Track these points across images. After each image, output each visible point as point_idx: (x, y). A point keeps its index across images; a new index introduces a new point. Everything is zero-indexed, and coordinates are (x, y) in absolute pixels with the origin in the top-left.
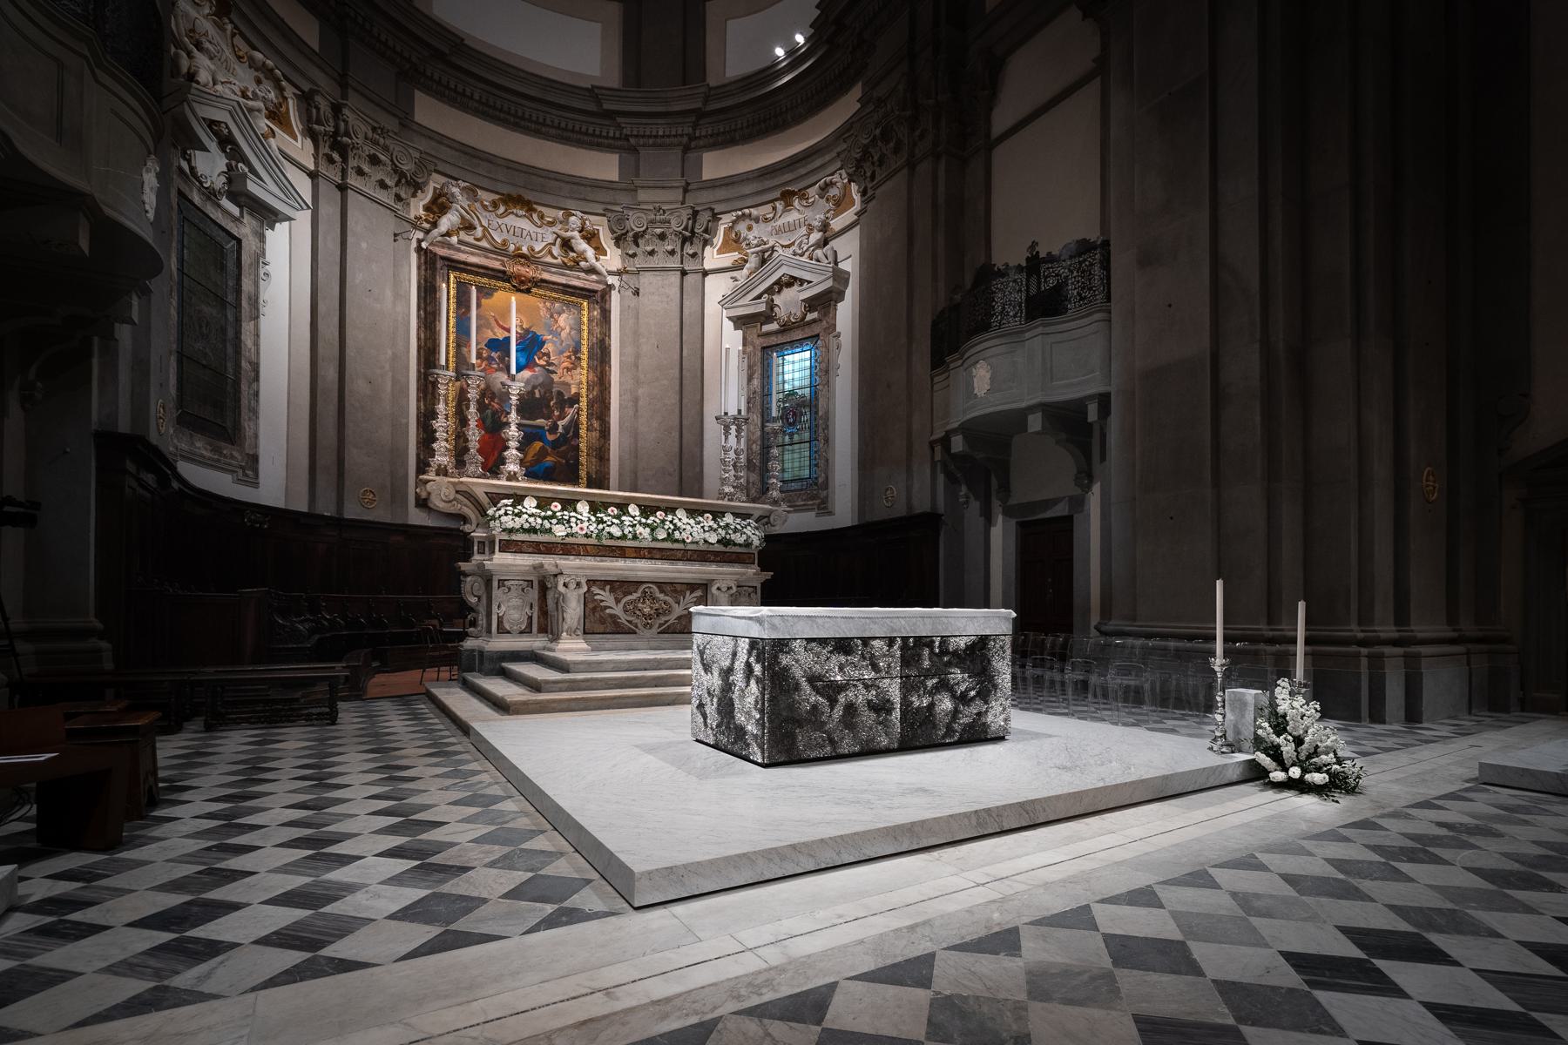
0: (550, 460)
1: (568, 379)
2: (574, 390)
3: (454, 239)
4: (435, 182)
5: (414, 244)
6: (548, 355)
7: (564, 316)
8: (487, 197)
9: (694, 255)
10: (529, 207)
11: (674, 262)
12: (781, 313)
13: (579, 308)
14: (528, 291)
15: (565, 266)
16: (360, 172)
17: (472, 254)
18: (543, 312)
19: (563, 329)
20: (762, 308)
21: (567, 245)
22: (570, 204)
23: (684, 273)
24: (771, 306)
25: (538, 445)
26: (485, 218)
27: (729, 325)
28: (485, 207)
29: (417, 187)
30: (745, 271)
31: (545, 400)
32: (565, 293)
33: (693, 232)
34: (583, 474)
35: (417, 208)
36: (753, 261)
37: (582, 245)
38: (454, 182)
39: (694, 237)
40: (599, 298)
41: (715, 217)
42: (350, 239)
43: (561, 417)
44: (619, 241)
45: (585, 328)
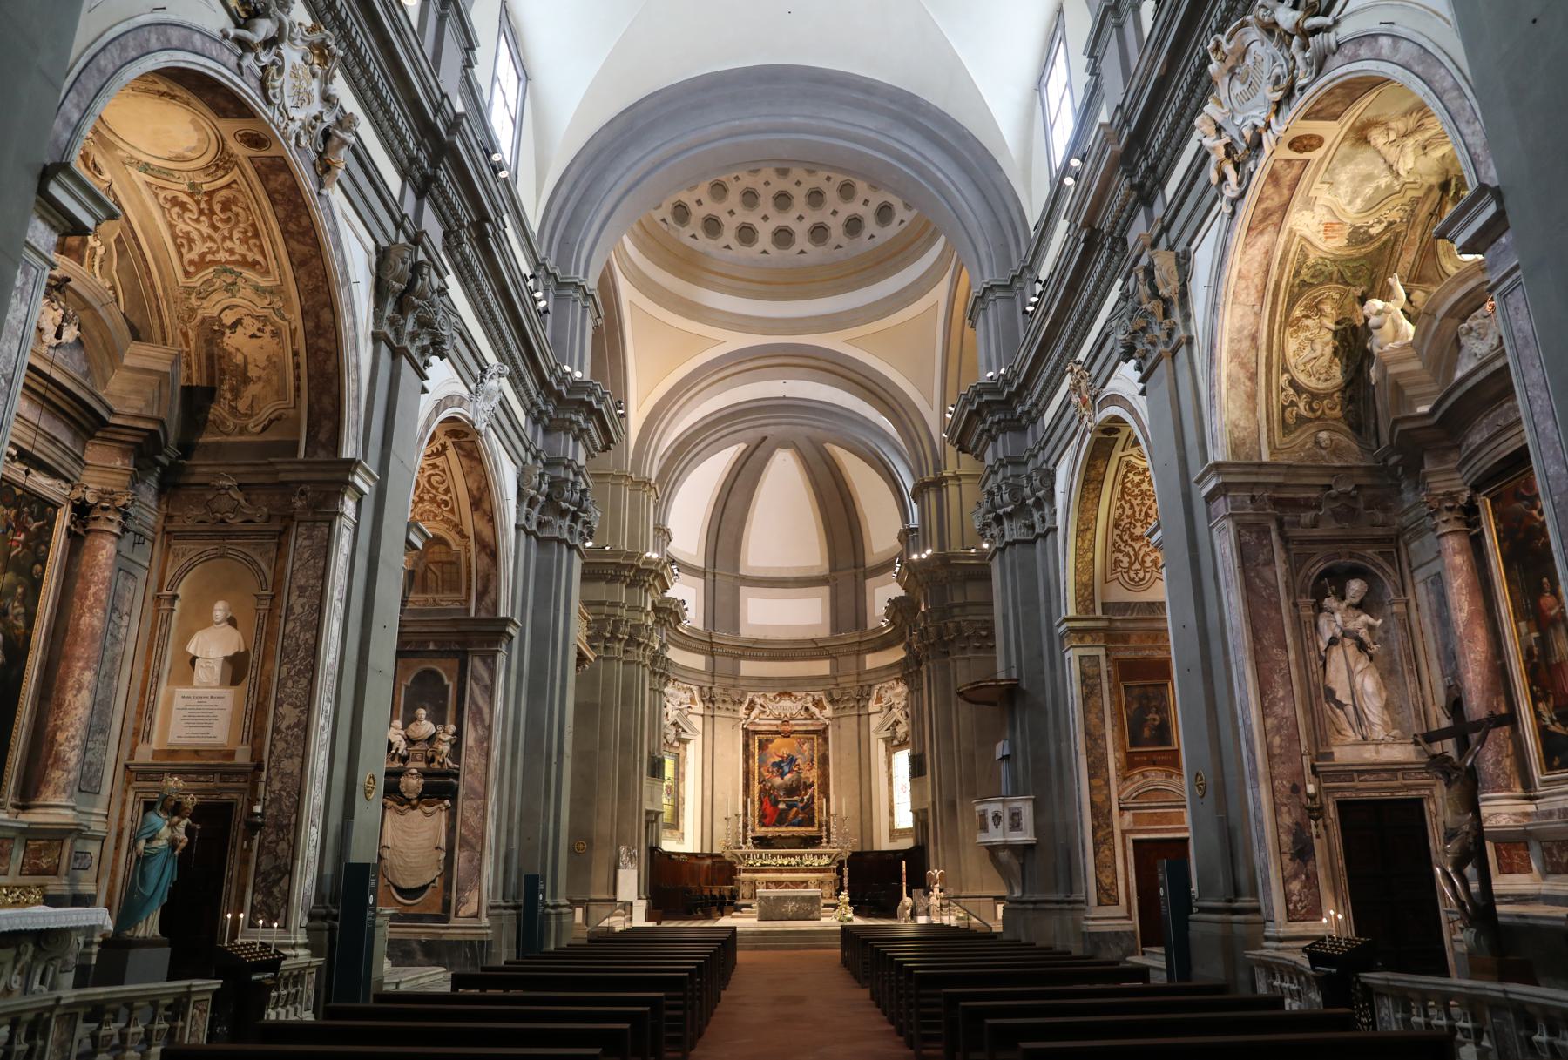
0: (800, 816)
4: (750, 696)
8: (770, 695)
10: (790, 695)
11: (855, 712)
12: (899, 735)
18: (796, 745)
20: (889, 734)
21: (807, 709)
26: (770, 706)
27: (881, 741)
29: (741, 703)
30: (882, 715)
31: (798, 787)
35: (742, 711)
36: (885, 710)
37: (813, 709)
39: (863, 697)
40: (822, 733)
41: (871, 686)
44: (832, 702)
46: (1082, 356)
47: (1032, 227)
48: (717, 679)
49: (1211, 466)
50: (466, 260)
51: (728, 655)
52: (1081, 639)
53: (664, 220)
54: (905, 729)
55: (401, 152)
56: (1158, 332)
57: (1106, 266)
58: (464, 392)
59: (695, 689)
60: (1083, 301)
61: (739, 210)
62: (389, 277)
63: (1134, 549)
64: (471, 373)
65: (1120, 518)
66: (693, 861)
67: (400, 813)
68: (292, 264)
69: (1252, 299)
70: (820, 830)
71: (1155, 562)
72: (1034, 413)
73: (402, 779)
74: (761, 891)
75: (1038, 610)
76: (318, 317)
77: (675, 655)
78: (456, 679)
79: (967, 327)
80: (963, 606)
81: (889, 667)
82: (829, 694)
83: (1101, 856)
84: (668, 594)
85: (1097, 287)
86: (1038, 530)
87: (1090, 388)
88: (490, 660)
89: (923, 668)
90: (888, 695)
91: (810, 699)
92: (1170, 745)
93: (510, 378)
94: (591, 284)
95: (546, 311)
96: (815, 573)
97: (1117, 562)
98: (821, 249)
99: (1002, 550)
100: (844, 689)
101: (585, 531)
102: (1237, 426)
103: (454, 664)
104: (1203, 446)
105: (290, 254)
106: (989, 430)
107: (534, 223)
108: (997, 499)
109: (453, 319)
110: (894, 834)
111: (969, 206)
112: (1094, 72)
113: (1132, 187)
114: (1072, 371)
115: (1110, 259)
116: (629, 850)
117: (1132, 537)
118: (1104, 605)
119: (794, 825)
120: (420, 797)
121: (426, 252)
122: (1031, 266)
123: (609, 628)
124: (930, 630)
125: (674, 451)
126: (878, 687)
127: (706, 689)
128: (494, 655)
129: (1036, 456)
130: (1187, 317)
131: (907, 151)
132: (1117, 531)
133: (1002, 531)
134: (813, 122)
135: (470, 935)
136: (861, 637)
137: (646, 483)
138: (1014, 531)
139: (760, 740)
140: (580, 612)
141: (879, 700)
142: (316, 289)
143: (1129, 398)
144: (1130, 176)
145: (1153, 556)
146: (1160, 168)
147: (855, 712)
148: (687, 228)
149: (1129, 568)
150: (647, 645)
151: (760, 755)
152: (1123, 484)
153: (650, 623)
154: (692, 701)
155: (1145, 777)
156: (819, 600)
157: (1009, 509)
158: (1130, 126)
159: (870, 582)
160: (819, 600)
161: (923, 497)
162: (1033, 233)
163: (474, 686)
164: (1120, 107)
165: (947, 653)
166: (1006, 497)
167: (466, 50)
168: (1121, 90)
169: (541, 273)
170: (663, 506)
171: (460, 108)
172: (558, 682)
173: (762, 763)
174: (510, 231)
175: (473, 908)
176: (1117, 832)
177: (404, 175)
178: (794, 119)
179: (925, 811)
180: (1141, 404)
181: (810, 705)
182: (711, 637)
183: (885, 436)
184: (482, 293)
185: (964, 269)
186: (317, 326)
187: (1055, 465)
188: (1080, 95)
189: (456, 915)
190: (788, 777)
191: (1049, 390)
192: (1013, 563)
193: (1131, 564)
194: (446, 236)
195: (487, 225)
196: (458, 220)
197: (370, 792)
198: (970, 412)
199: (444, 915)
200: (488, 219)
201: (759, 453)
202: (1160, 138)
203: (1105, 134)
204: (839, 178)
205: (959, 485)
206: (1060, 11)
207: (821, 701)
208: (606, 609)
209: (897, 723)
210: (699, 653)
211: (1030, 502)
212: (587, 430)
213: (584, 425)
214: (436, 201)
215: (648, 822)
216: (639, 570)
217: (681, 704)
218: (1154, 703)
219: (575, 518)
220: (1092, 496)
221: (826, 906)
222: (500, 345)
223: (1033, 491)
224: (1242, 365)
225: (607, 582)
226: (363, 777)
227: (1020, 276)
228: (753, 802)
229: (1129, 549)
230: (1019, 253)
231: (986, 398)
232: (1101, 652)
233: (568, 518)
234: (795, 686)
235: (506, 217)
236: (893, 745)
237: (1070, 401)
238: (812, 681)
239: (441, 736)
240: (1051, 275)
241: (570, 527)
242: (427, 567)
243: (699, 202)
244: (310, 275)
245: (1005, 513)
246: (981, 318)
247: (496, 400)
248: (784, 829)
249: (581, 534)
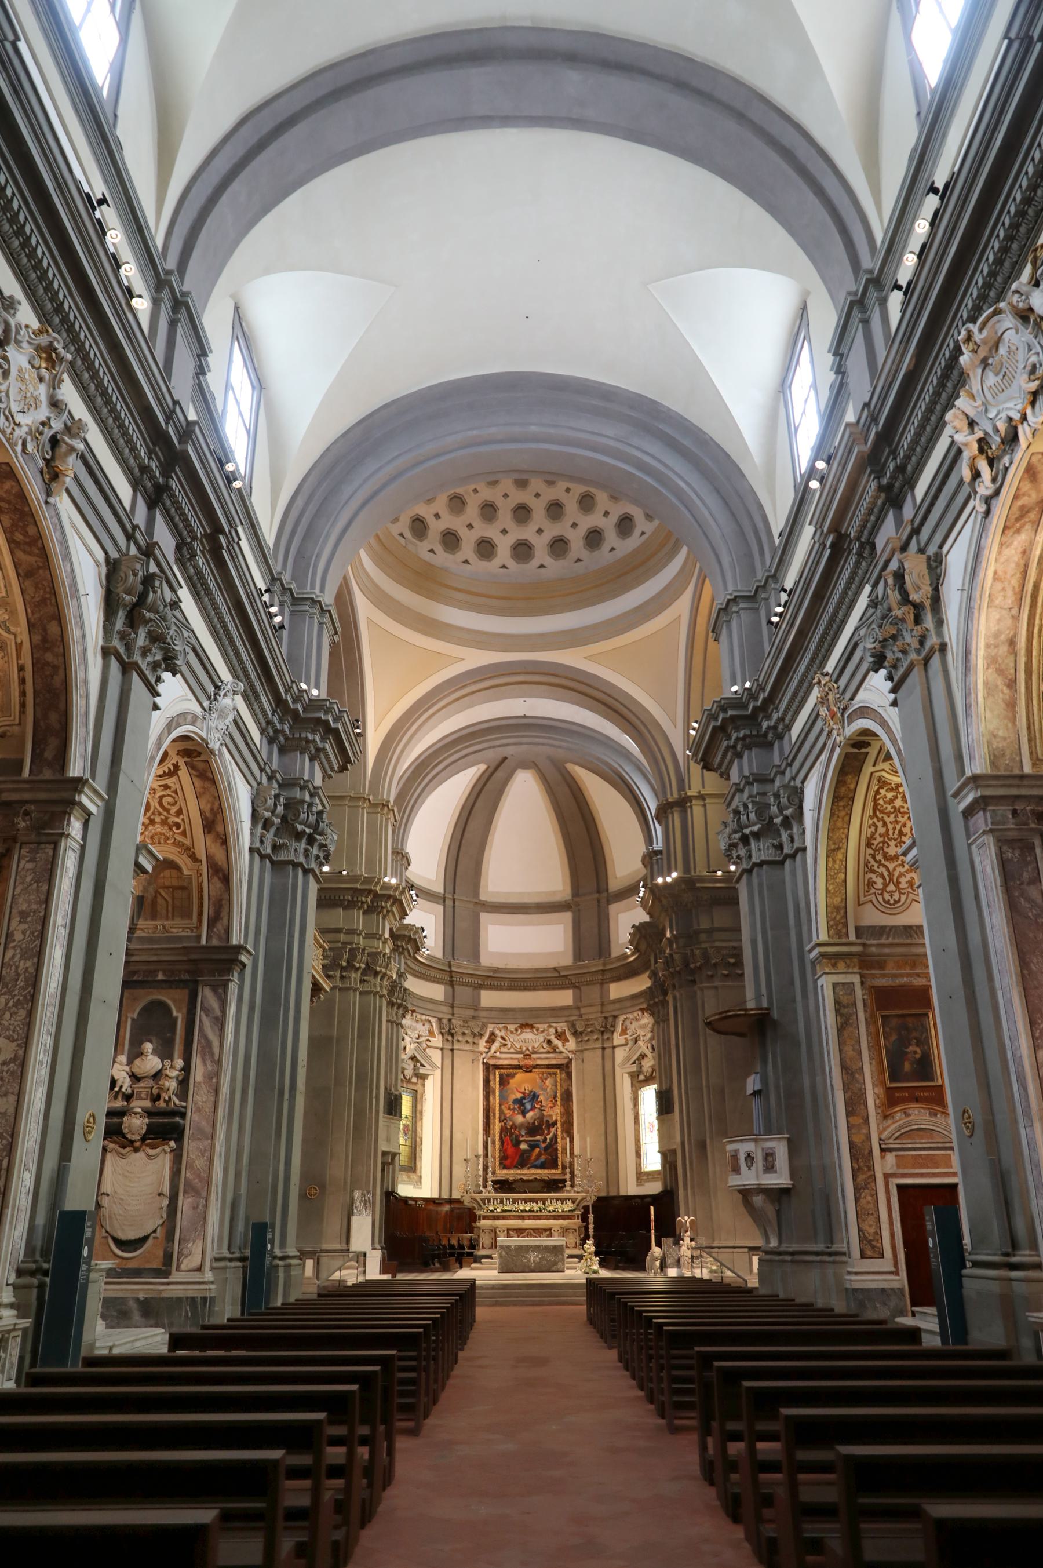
0: (543, 1158)
1: (551, 1113)
2: (554, 1118)
3: (498, 1054)
4: (490, 1028)
5: (481, 1061)
6: (541, 1102)
7: (548, 1080)
8: (512, 1027)
9: (608, 1039)
10: (531, 1027)
11: (599, 1045)
12: (645, 1069)
13: (555, 1074)
14: (531, 1071)
15: (548, 1052)
16: (458, 1041)
17: (506, 1059)
18: (539, 1080)
20: (634, 1068)
21: (549, 1042)
22: (551, 1020)
23: (604, 1049)
24: (641, 1066)
25: (537, 1150)
26: (511, 1038)
27: (626, 1076)
28: (512, 1032)
29: (481, 1035)
30: (627, 1048)
32: (548, 1068)
33: (606, 1027)
34: (560, 1163)
35: (482, 1043)
36: (631, 1043)
37: (556, 1042)
38: (497, 1026)
39: (607, 1029)
40: (565, 1068)
41: (615, 1017)
43: (548, 1134)
44: (575, 1034)
45: (558, 1084)
46: (830, 666)
47: (776, 535)
48: (456, 1010)
49: (969, 779)
50: (199, 573)
51: (467, 985)
52: (834, 966)
53: (401, 535)
54: (652, 1063)
55: (132, 461)
56: (909, 639)
57: (854, 573)
58: (197, 709)
59: (433, 1020)
60: (830, 610)
61: (477, 523)
62: (120, 589)
63: (888, 870)
64: (204, 690)
65: (872, 836)
66: (431, 1207)
67: (122, 1156)
68: (18, 575)
69: (1010, 600)
70: (564, 1174)
71: (911, 883)
72: (780, 727)
73: (125, 1119)
74: (502, 1240)
75: (788, 934)
76: (45, 630)
77: (413, 984)
78: (185, 1010)
79: (711, 640)
80: (710, 932)
81: (634, 997)
82: (572, 1024)
83: (863, 1201)
84: (406, 921)
85: (844, 593)
86: (786, 850)
87: (838, 701)
88: (221, 989)
89: (670, 998)
90: (633, 1026)
91: (552, 1031)
92: (933, 1080)
93: (245, 696)
94: (328, 599)
95: (282, 627)
96: (558, 898)
97: (871, 884)
98: (561, 563)
99: (749, 871)
100: (588, 1020)
101: (321, 855)
102: (995, 736)
103: (183, 994)
104: (959, 757)
105: (16, 565)
106: (734, 747)
107: (269, 536)
108: (744, 818)
109: (186, 634)
110: (642, 1176)
111: (710, 513)
112: (840, 370)
113: (880, 488)
114: (819, 683)
115: (857, 564)
116: (363, 1195)
117: (886, 857)
118: (858, 930)
119: (536, 1167)
120: (143, 1139)
121: (158, 565)
122: (776, 576)
123: (345, 957)
124: (676, 957)
125: (413, 772)
126: (622, 1018)
127: (445, 1021)
128: (225, 985)
129: (783, 773)
130: (940, 623)
131: (647, 459)
132: (869, 851)
133: (749, 851)
134: (552, 431)
135: (192, 1291)
136: (604, 965)
137: (384, 806)
138: (761, 851)
139: (501, 1075)
140: (316, 939)
141: (624, 1032)
142: (43, 601)
143: (880, 710)
144: (878, 478)
145: (908, 877)
146: (909, 468)
147: (599, 1045)
148: (425, 542)
149: (884, 890)
150: (385, 974)
151: (501, 1091)
152: (875, 800)
153: (387, 951)
154: (431, 1033)
155: (907, 1115)
156: (561, 927)
157: (756, 828)
158: (877, 425)
159: (613, 908)
160: (561, 927)
161: (667, 818)
162: (777, 541)
163: (204, 1018)
164: (867, 405)
165: (694, 982)
166: (752, 816)
167: (199, 356)
168: (867, 388)
169: (277, 588)
170: (401, 829)
171: (192, 416)
172: (292, 1013)
173: (503, 1099)
174: (244, 543)
175: (195, 1261)
176: (879, 1177)
177: (135, 484)
178: (533, 428)
179: (674, 1152)
180: (892, 715)
181: (552, 1038)
182: (450, 966)
183: (627, 755)
184: (216, 608)
185: (707, 582)
186: (45, 640)
187: (803, 782)
188: (825, 394)
189: (178, 1269)
190: (530, 1115)
191: (796, 703)
192: (760, 885)
193: (886, 885)
194: (179, 548)
195: (221, 537)
196: (191, 531)
197: (90, 1132)
198: (714, 728)
199: (163, 1272)
200: (221, 531)
201: (500, 774)
202: (909, 436)
203: (851, 434)
204: (579, 489)
205: (704, 806)
206: (804, 309)
207: (564, 1033)
208: (342, 937)
209: (643, 1056)
210: (438, 983)
211: (778, 820)
212: (324, 750)
213: (320, 745)
214: (168, 512)
215: (383, 1164)
216: (376, 895)
217: (419, 1036)
218: (914, 1034)
219: (311, 841)
220: (842, 813)
221: (571, 1256)
222: (235, 661)
223: (781, 809)
224: (1000, 672)
225: (345, 908)
226: (82, 1116)
227: (764, 586)
228: (493, 1143)
229: (882, 870)
230: (763, 562)
231: (730, 713)
232: (856, 979)
233: (304, 841)
234: (537, 1017)
235: (240, 529)
236: (639, 1081)
237: (818, 714)
238: (555, 1012)
239: (168, 1072)
240: (797, 584)
241: (306, 851)
242: (157, 892)
243: (437, 516)
244: (36, 587)
245: (752, 833)
246: (724, 631)
247: (230, 718)
248: (525, 1171)
249: (317, 857)
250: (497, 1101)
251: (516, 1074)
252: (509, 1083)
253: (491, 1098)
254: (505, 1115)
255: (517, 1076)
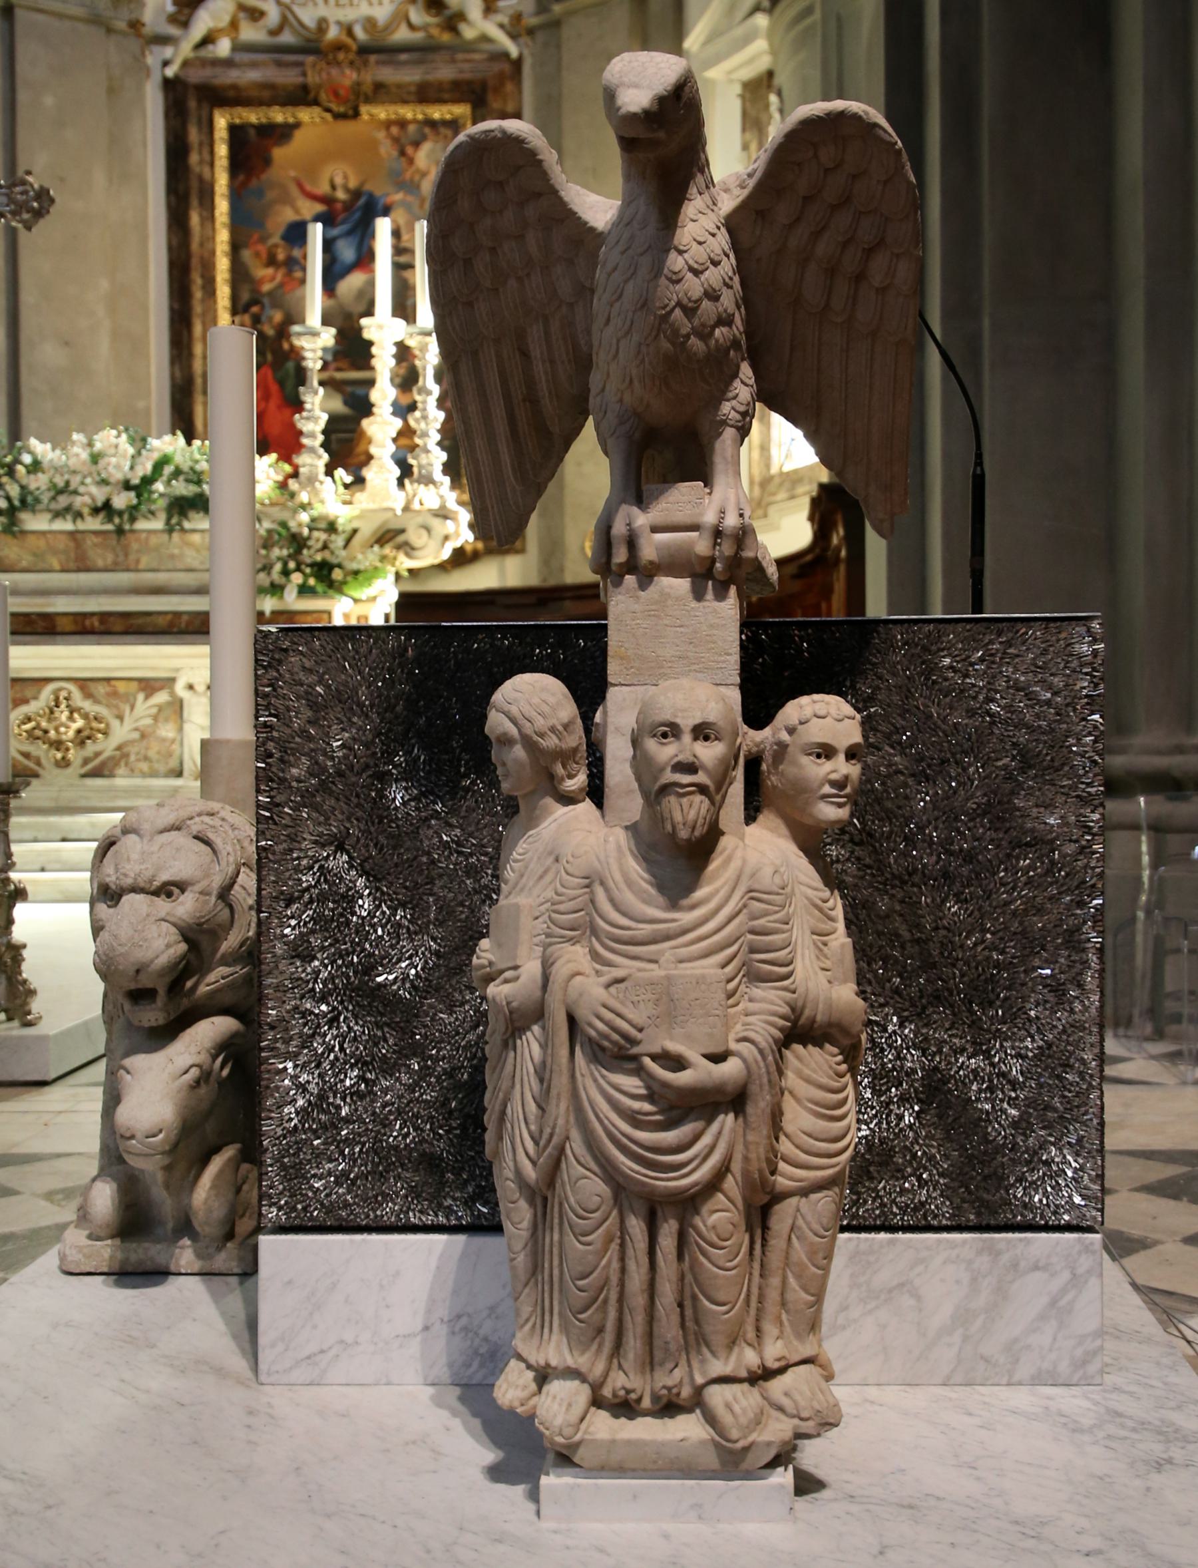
7: (426, 147)
17: (254, 65)
18: (387, 149)
19: (424, 174)
42: (23, 96)
139: (235, 131)
151: (236, 196)
250: (223, 237)
251: (297, 125)
252: (267, 162)
253: (195, 219)
254: (255, 284)
255: (299, 135)
